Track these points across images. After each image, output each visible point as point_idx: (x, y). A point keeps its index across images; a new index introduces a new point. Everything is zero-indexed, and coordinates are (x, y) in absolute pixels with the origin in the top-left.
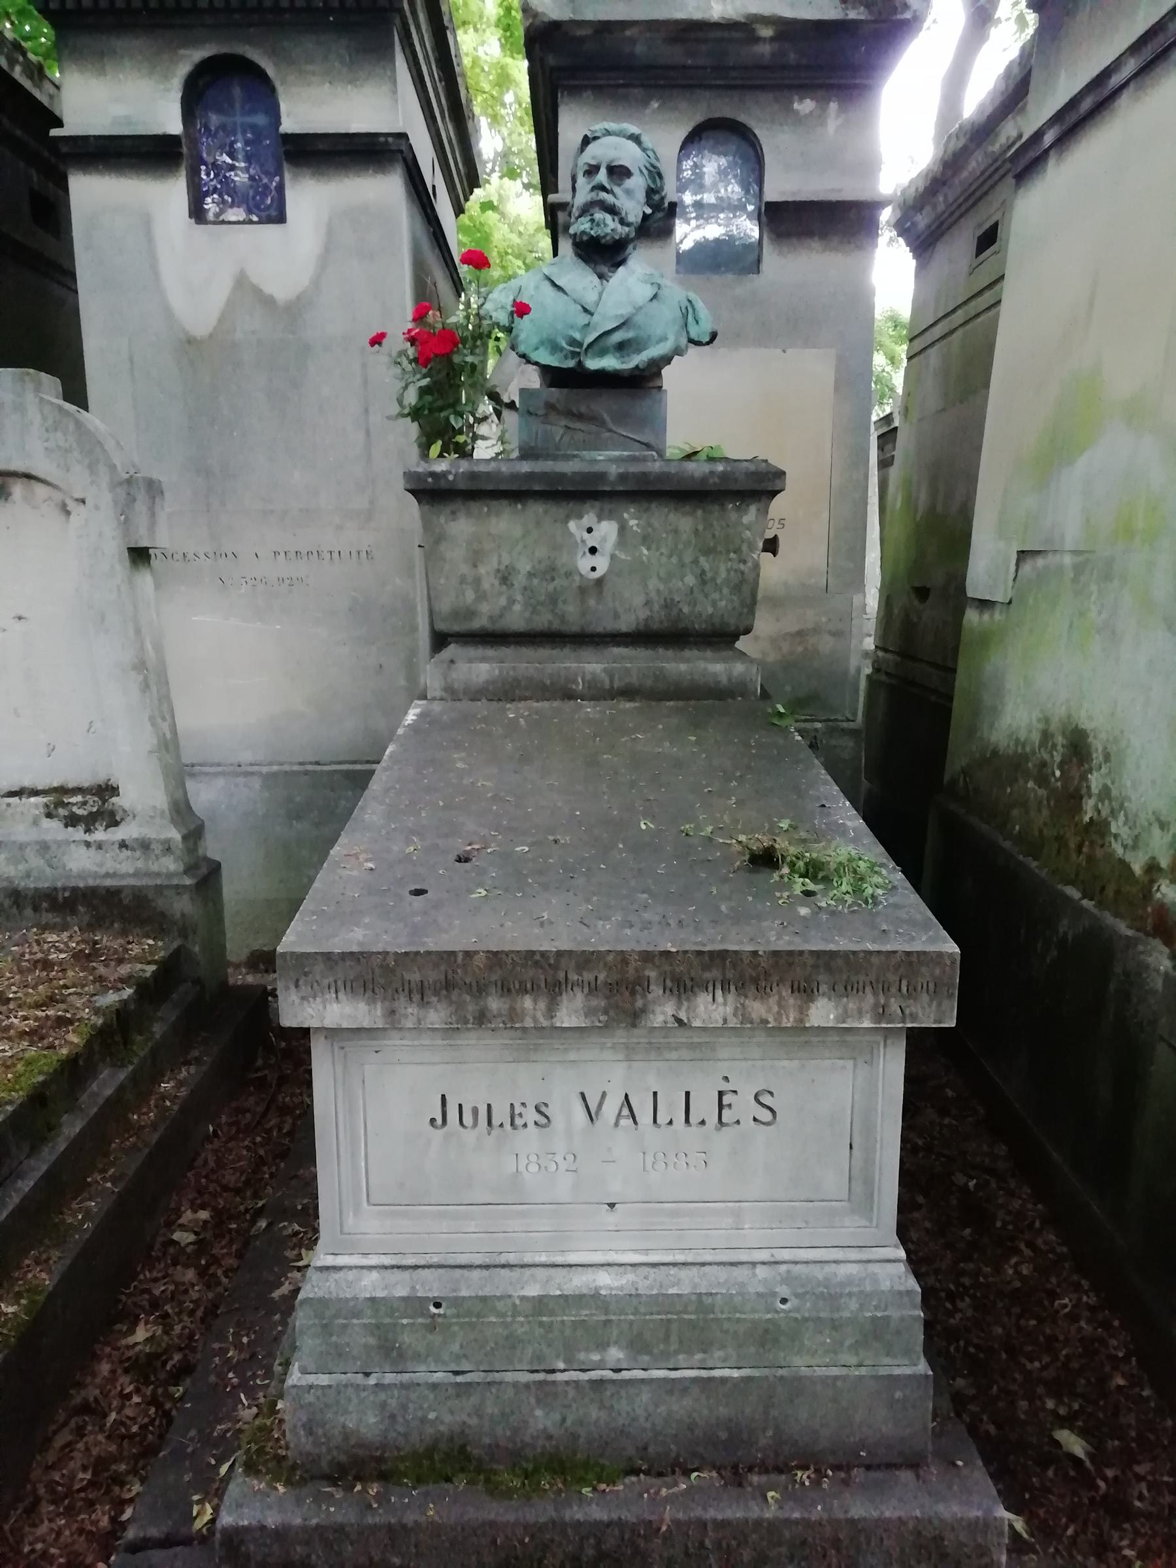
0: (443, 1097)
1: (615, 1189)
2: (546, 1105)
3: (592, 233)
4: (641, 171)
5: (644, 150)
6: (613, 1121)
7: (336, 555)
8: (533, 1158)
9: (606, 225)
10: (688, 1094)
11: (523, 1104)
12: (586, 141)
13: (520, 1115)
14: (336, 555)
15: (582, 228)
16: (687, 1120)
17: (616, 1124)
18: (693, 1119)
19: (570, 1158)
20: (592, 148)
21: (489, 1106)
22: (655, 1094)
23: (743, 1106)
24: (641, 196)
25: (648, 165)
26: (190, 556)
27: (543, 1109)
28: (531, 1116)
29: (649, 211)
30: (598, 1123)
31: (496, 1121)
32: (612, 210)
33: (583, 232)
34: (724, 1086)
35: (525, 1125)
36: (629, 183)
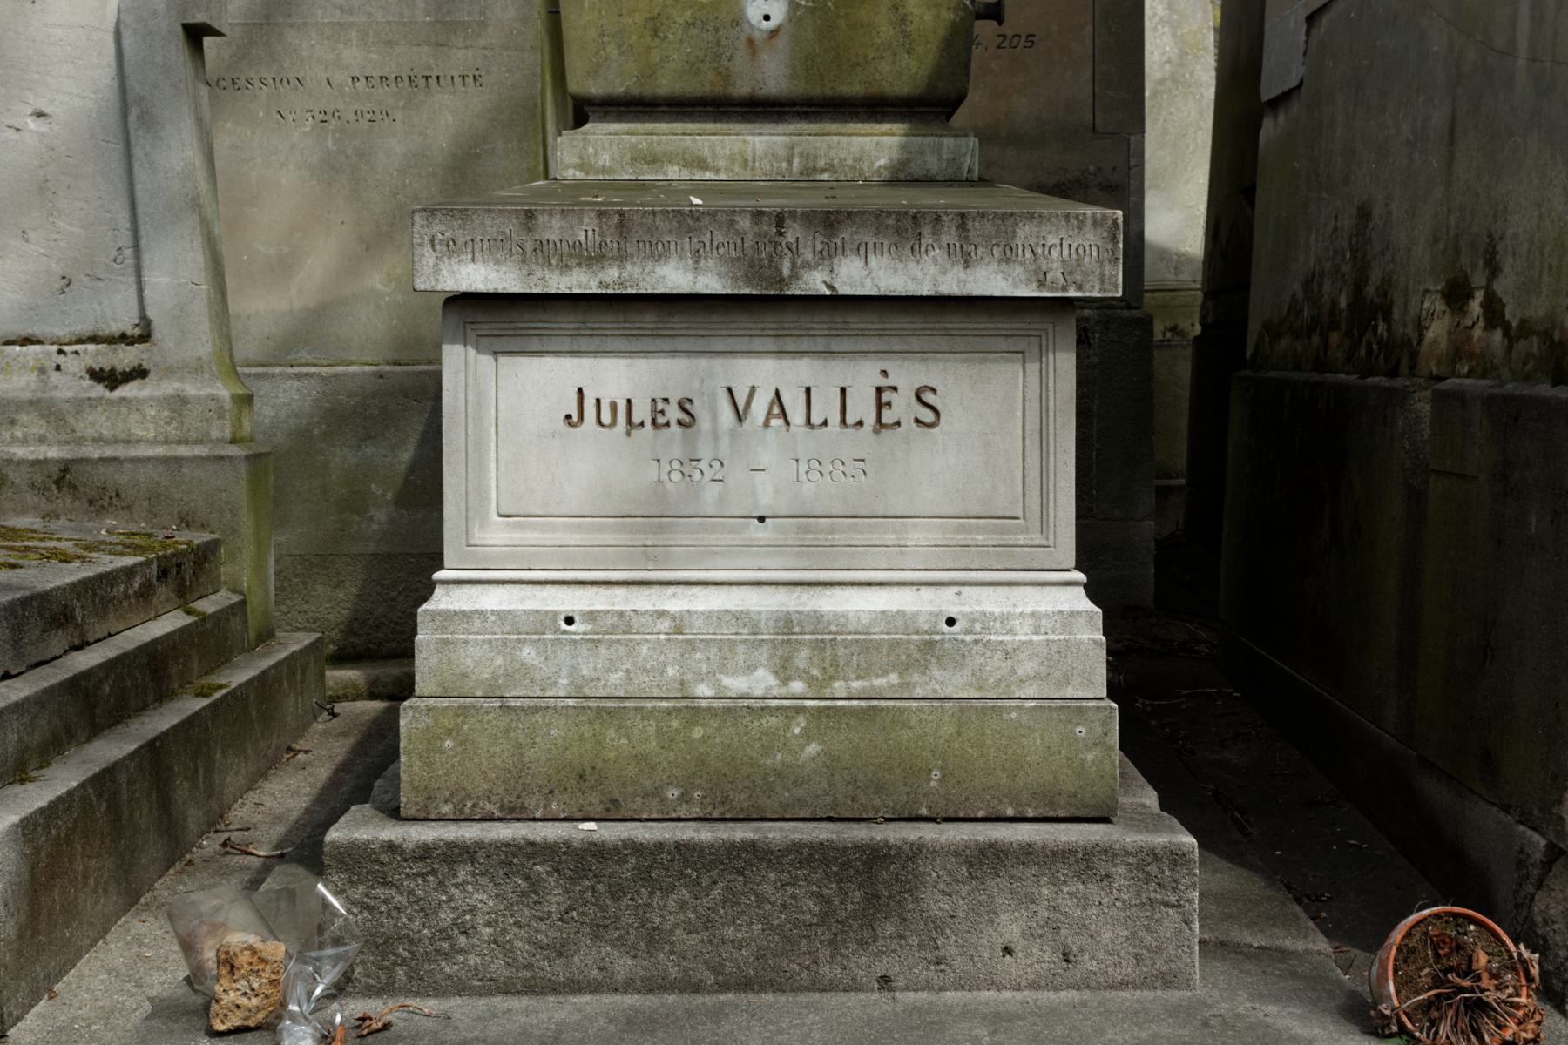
0: (580, 390)
1: (765, 503)
2: (690, 401)
6: (761, 419)
7: (433, 81)
8: (676, 465)
10: (843, 390)
11: (666, 400)
13: (662, 412)
14: (433, 81)
16: (843, 421)
17: (766, 424)
18: (850, 420)
19: (717, 464)
21: (629, 401)
22: (808, 390)
23: (902, 406)
26: (242, 83)
27: (687, 406)
28: (674, 413)
30: (746, 424)
31: (636, 419)
34: (883, 382)
35: (668, 424)
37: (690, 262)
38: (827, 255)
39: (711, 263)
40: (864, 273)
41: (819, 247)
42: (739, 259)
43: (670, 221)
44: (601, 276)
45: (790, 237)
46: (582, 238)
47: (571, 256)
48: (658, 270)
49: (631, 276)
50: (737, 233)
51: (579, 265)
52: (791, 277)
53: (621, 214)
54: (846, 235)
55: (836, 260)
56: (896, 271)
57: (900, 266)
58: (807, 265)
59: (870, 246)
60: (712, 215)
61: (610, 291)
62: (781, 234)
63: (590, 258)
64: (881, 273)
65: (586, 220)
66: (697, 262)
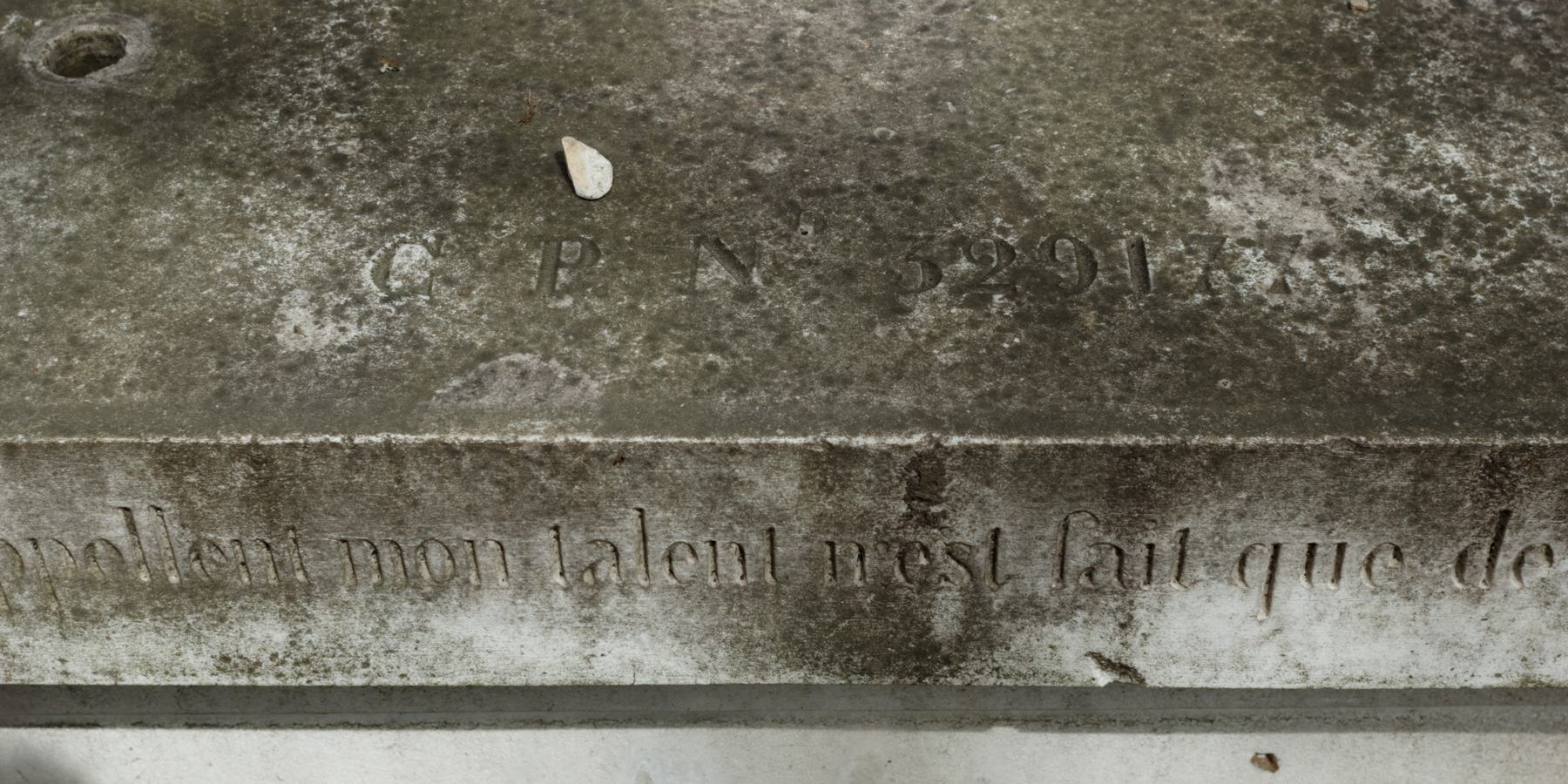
37: (562, 600)
38: (1120, 580)
39: (645, 603)
40: (1253, 631)
41: (1080, 557)
42: (758, 591)
43: (468, 481)
44: (218, 640)
45: (968, 530)
46: (115, 528)
47: (89, 584)
48: (437, 622)
49: (337, 642)
50: (747, 515)
51: (128, 608)
52: (961, 642)
53: (258, 458)
54: (1200, 524)
55: (1146, 596)
56: (1381, 623)
57: (1399, 610)
58: (1032, 610)
59: (1293, 556)
60: (648, 460)
61: (267, 680)
62: (929, 521)
63: (161, 589)
64: (1321, 632)
65: (115, 479)
66: (592, 601)
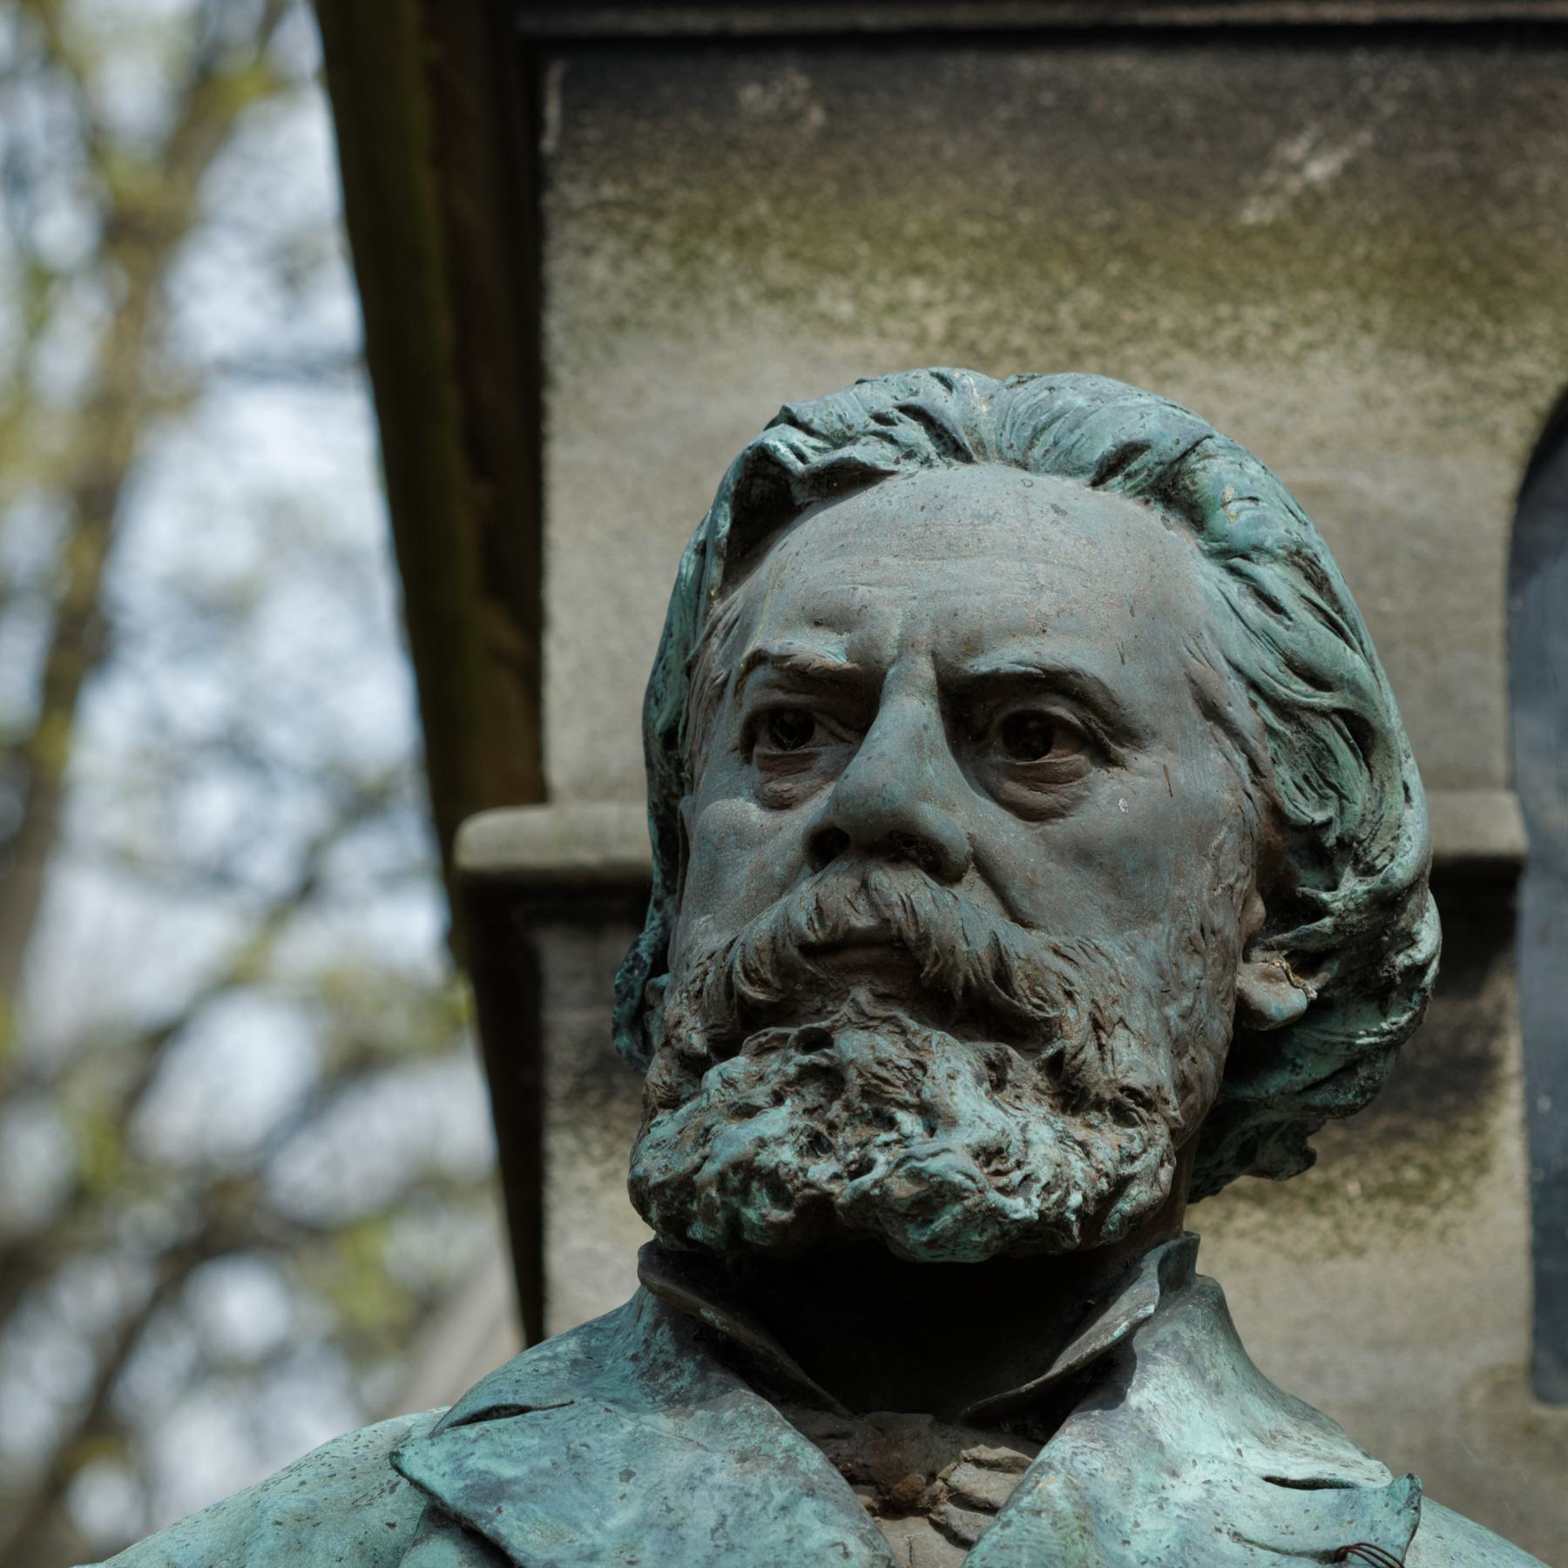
3: (821, 1170)
4: (1212, 711)
5: (1230, 556)
9: (933, 1116)
12: (766, 501)
15: (736, 1139)
20: (808, 553)
24: (1216, 885)
25: (1264, 664)
29: (1284, 997)
32: (990, 1012)
33: (747, 1173)
36: (1112, 798)
